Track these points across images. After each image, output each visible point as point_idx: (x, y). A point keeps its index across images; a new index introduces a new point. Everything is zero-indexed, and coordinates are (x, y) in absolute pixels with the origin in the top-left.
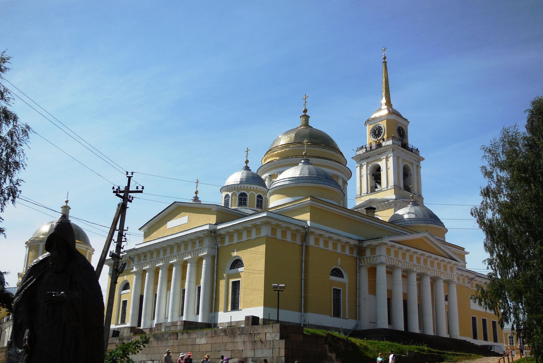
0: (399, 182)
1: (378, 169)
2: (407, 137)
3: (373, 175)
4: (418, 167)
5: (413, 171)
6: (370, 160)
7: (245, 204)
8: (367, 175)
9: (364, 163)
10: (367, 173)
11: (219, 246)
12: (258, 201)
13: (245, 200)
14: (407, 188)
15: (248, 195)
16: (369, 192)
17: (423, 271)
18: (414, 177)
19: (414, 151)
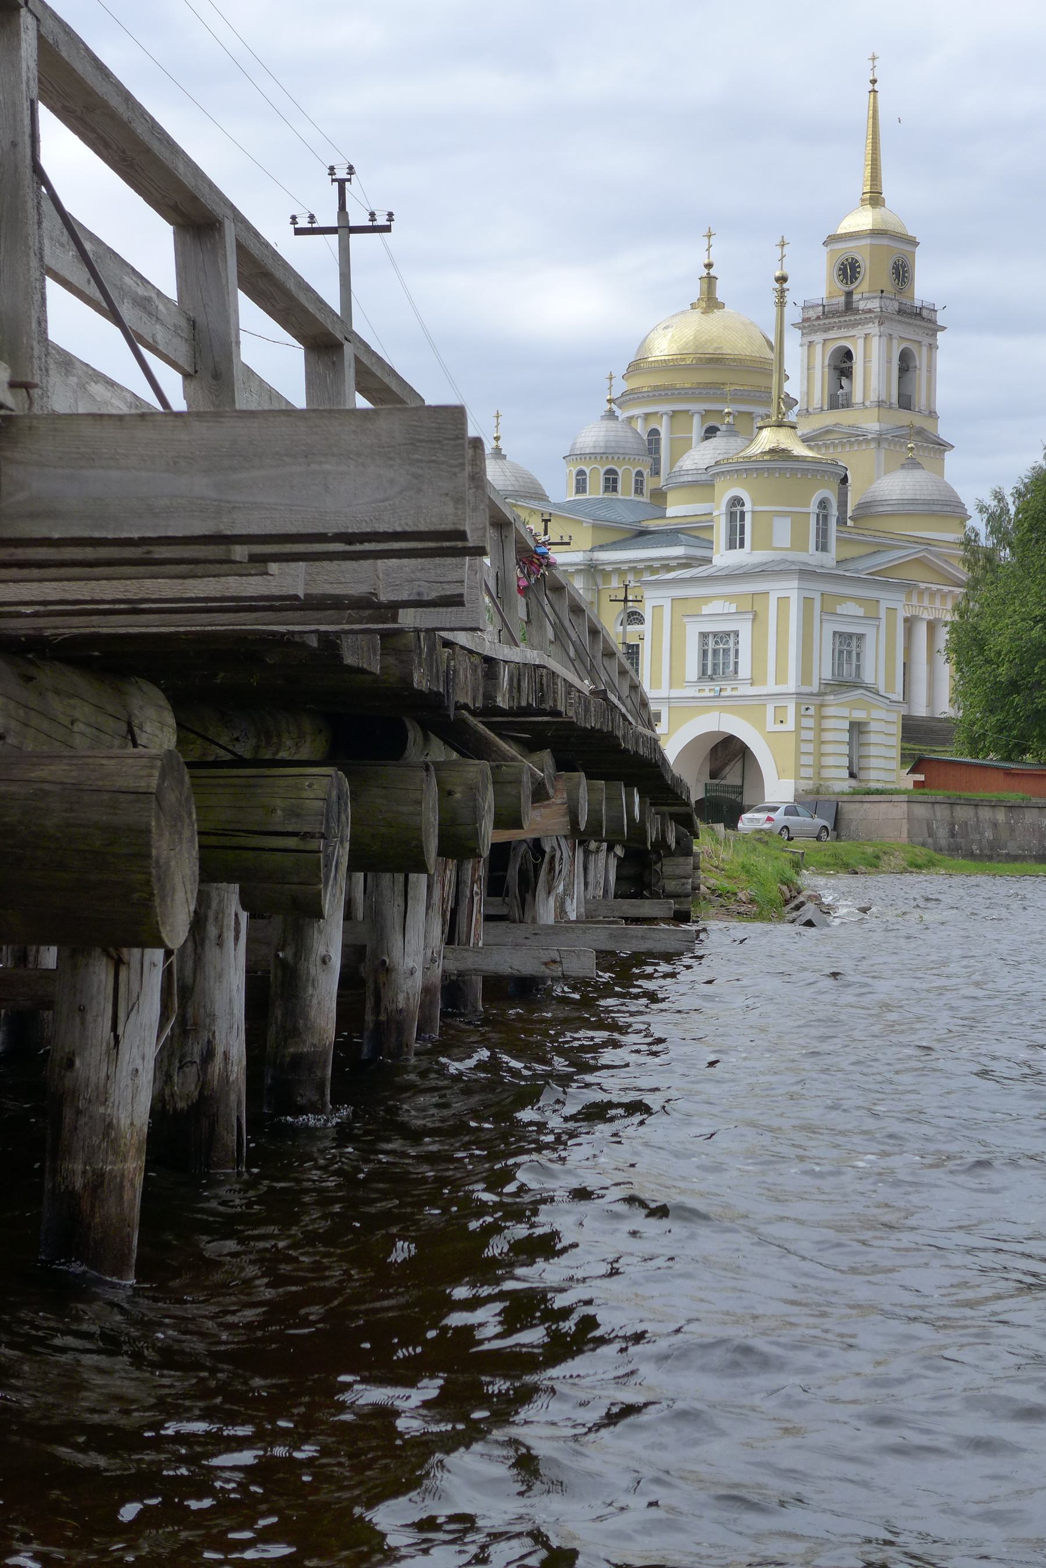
0: (889, 395)
1: (848, 355)
2: (913, 279)
3: (836, 368)
4: (932, 347)
5: (921, 359)
6: (831, 335)
7: (615, 489)
8: (823, 367)
9: (818, 337)
10: (823, 363)
11: (601, 587)
12: (636, 481)
13: (615, 481)
14: (905, 402)
15: (620, 474)
16: (825, 408)
17: (915, 612)
18: (921, 376)
19: (925, 313)
